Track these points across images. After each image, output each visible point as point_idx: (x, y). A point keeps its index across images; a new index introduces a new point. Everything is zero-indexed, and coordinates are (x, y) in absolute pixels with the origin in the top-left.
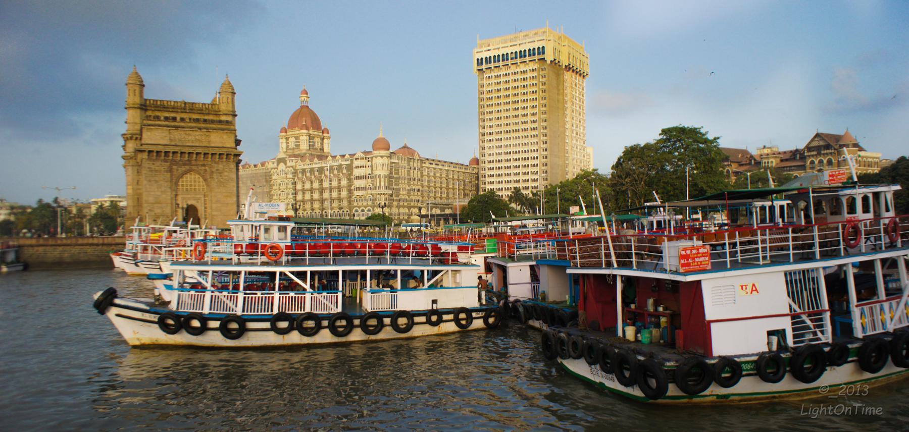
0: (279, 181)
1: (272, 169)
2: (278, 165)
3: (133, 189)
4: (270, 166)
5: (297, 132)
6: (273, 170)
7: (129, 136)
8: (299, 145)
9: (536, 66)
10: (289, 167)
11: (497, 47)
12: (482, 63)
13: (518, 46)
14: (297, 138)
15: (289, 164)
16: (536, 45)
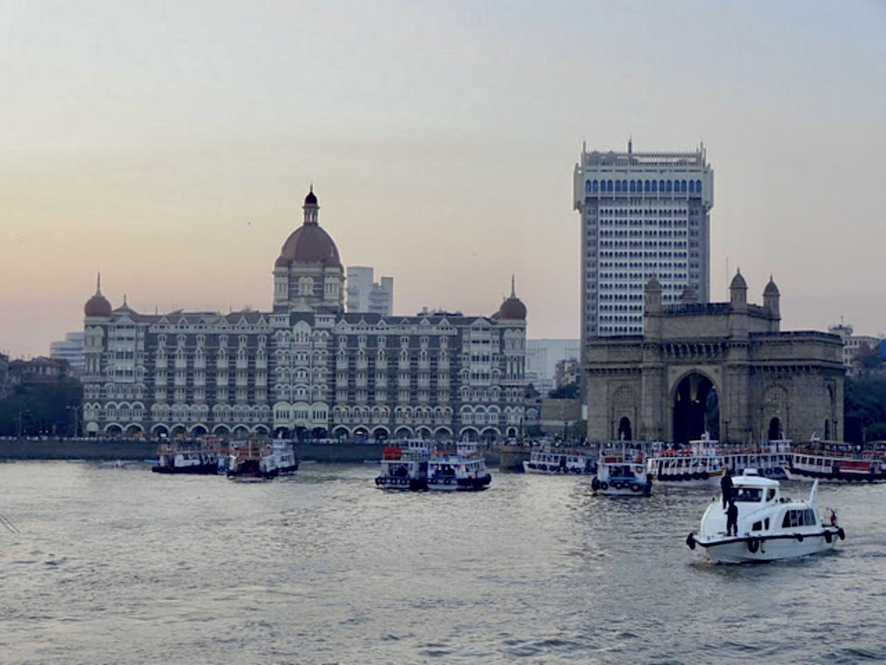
0: (292, 353)
1: (276, 329)
2: (293, 322)
4: (274, 323)
5: (318, 270)
6: (280, 331)
7: (746, 344)
8: (323, 292)
9: (685, 207)
10: (320, 329)
11: (624, 168)
12: (596, 190)
13: (658, 173)
14: (315, 279)
15: (318, 324)
16: (688, 177)
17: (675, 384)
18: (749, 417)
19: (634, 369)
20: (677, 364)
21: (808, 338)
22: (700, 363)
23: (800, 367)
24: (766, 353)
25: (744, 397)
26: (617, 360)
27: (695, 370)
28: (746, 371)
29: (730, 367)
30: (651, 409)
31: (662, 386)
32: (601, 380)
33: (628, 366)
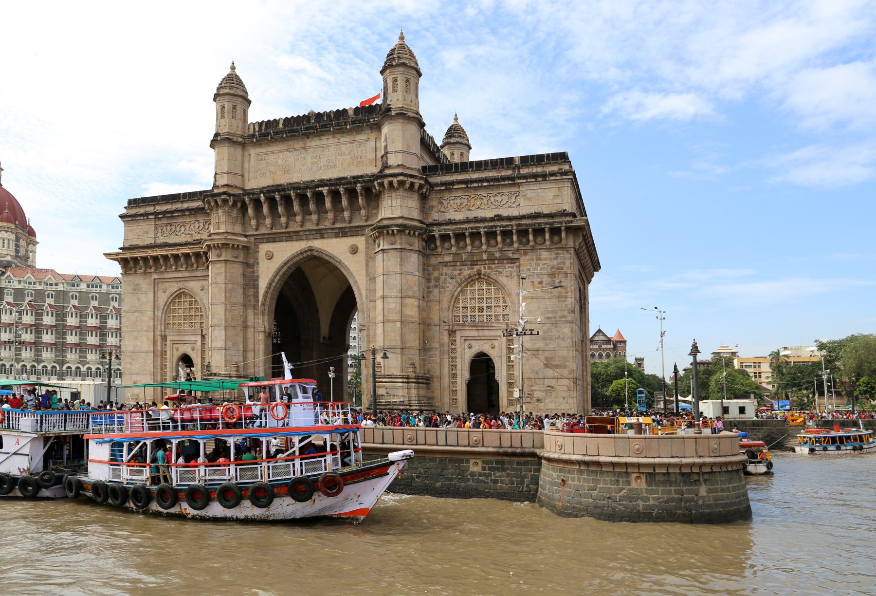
3: (419, 307)
17: (272, 281)
18: (425, 349)
19: (197, 255)
20: (274, 241)
21: (555, 168)
22: (320, 234)
23: (539, 232)
24: (459, 209)
25: (413, 302)
26: (171, 240)
27: (311, 249)
28: (417, 244)
29: (382, 230)
30: (223, 333)
31: (245, 287)
32: (144, 283)
33: (186, 250)
